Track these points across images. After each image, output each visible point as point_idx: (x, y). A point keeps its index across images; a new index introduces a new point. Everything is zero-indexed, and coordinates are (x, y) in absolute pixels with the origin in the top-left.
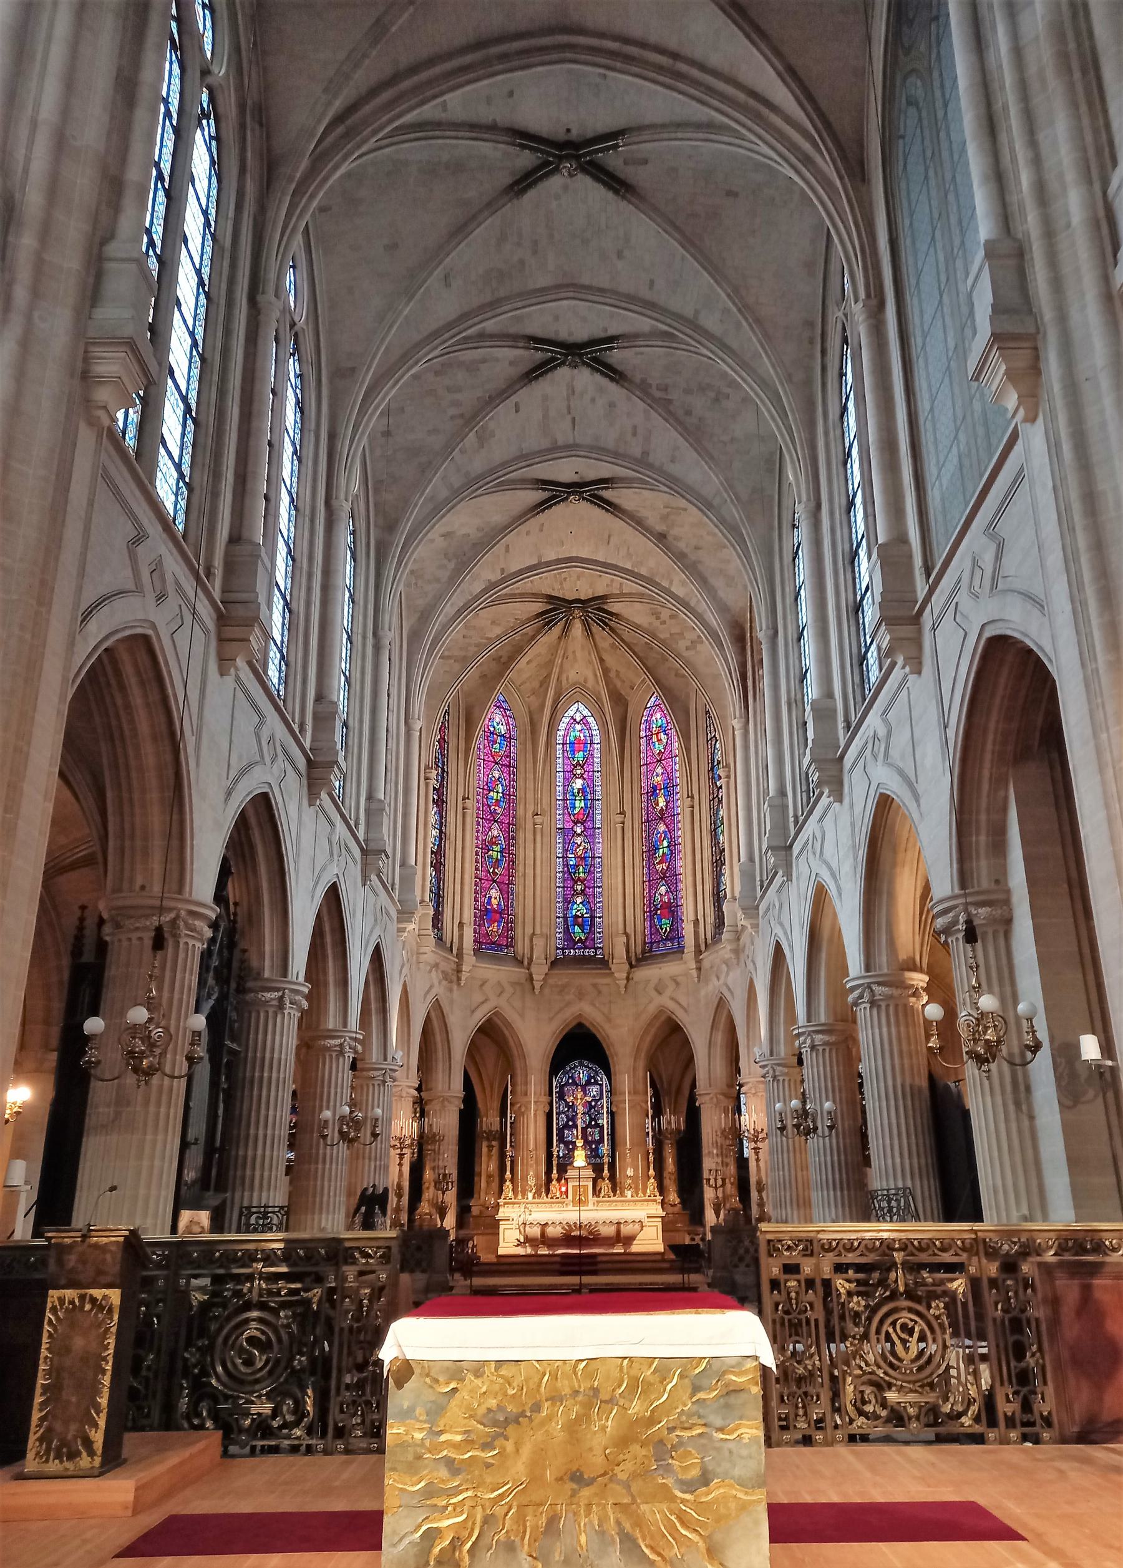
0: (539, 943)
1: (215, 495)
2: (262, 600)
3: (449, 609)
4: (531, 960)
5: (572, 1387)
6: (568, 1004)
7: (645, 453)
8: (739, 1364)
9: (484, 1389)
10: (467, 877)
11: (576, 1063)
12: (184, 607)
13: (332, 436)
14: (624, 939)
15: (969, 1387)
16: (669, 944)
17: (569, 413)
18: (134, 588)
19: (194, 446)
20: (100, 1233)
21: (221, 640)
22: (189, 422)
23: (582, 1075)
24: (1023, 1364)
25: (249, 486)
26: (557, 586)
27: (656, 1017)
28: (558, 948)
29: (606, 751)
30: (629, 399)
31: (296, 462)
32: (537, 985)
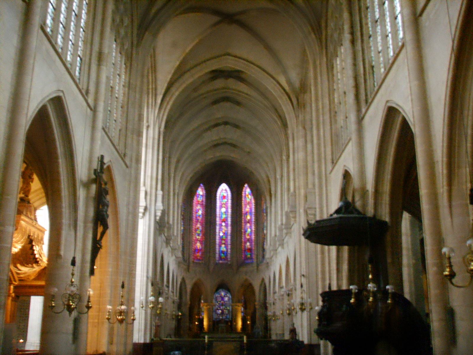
23: (223, 294)
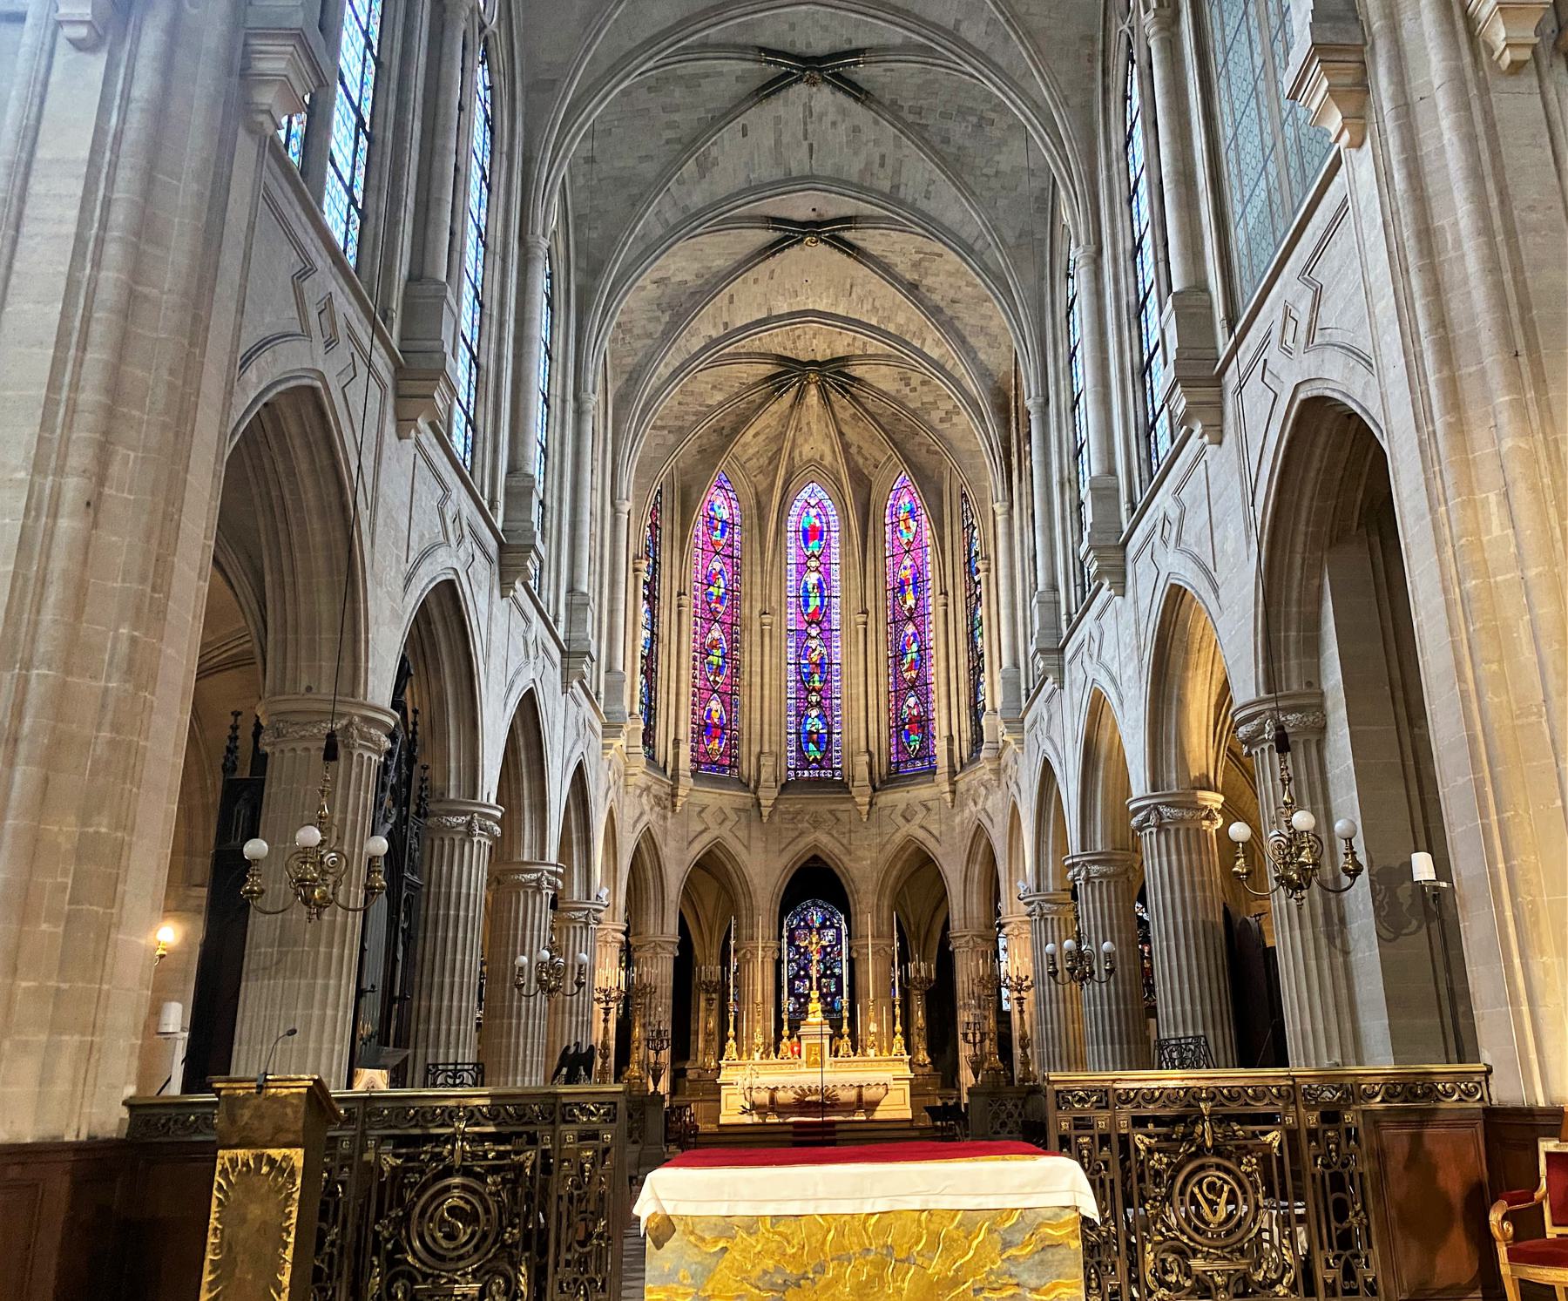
0: (768, 762)
1: (393, 223)
2: (448, 349)
3: (663, 371)
4: (758, 782)
5: (861, 1245)
6: (801, 834)
7: (895, 187)
8: (1056, 1216)
9: (759, 1248)
10: (683, 686)
11: (809, 902)
12: (356, 355)
13: (528, 161)
14: (866, 758)
15: (1284, 1251)
16: (919, 764)
17: (806, 139)
18: (300, 331)
19: (367, 166)
20: (278, 1084)
21: (398, 396)
22: (362, 138)
23: (816, 918)
24: (1346, 1225)
25: (432, 215)
26: (789, 345)
27: (903, 849)
28: (789, 769)
29: (846, 540)
30: (876, 122)
31: (485, 190)
32: (766, 812)
